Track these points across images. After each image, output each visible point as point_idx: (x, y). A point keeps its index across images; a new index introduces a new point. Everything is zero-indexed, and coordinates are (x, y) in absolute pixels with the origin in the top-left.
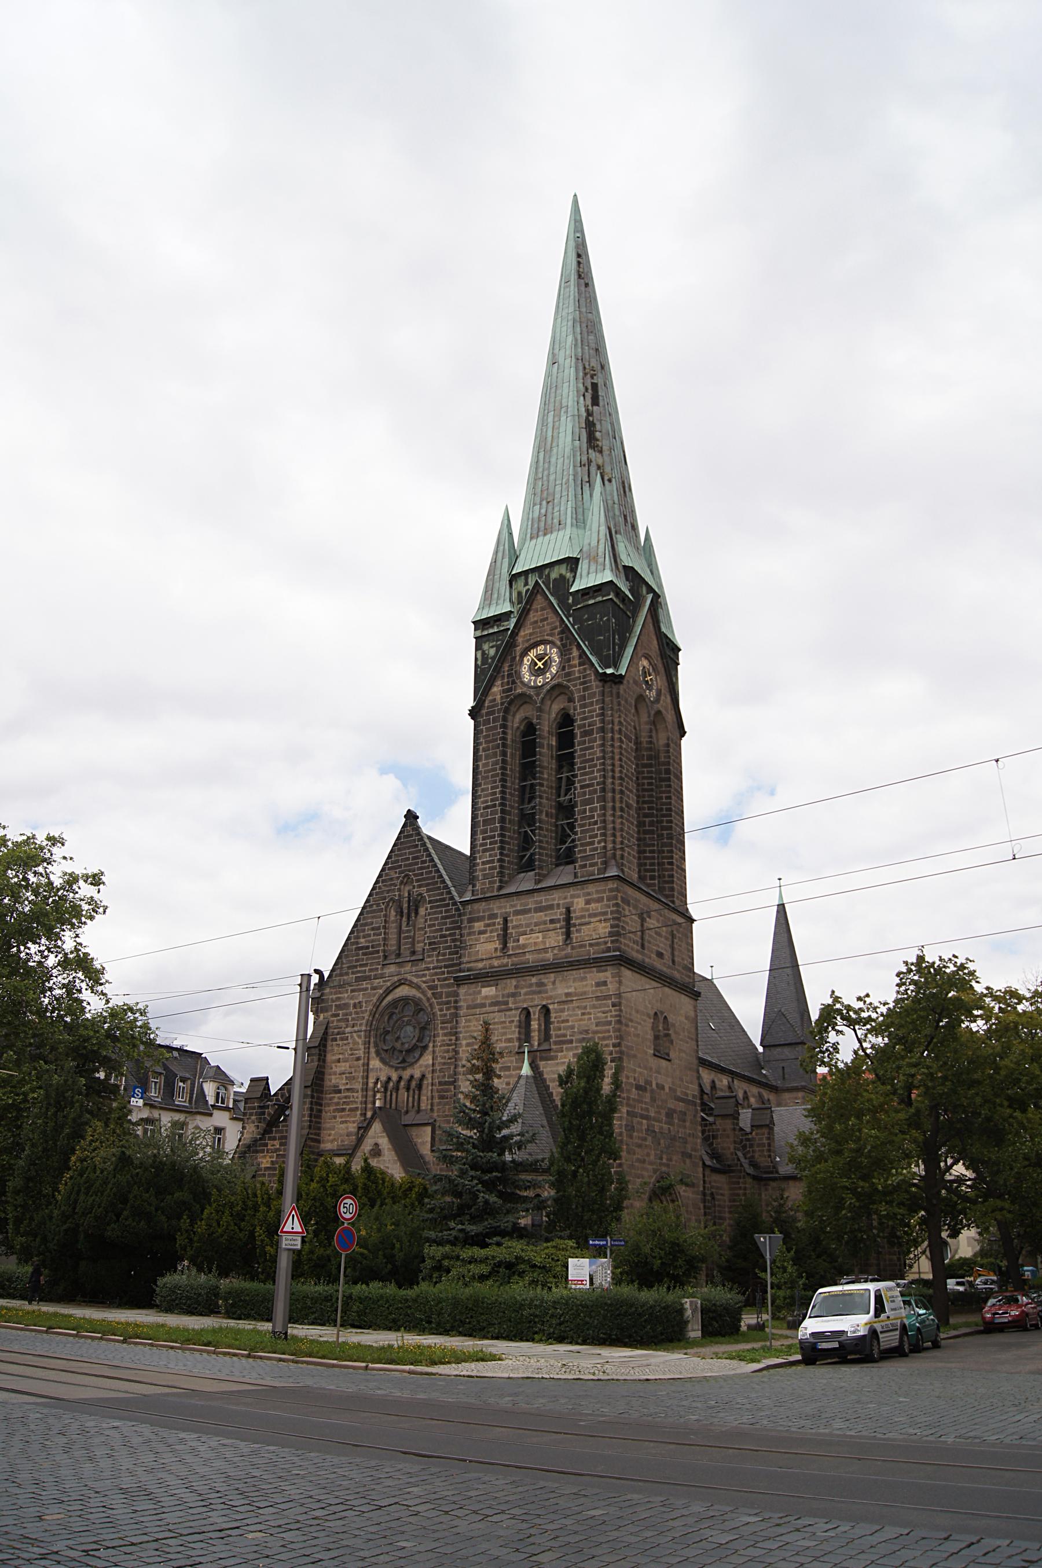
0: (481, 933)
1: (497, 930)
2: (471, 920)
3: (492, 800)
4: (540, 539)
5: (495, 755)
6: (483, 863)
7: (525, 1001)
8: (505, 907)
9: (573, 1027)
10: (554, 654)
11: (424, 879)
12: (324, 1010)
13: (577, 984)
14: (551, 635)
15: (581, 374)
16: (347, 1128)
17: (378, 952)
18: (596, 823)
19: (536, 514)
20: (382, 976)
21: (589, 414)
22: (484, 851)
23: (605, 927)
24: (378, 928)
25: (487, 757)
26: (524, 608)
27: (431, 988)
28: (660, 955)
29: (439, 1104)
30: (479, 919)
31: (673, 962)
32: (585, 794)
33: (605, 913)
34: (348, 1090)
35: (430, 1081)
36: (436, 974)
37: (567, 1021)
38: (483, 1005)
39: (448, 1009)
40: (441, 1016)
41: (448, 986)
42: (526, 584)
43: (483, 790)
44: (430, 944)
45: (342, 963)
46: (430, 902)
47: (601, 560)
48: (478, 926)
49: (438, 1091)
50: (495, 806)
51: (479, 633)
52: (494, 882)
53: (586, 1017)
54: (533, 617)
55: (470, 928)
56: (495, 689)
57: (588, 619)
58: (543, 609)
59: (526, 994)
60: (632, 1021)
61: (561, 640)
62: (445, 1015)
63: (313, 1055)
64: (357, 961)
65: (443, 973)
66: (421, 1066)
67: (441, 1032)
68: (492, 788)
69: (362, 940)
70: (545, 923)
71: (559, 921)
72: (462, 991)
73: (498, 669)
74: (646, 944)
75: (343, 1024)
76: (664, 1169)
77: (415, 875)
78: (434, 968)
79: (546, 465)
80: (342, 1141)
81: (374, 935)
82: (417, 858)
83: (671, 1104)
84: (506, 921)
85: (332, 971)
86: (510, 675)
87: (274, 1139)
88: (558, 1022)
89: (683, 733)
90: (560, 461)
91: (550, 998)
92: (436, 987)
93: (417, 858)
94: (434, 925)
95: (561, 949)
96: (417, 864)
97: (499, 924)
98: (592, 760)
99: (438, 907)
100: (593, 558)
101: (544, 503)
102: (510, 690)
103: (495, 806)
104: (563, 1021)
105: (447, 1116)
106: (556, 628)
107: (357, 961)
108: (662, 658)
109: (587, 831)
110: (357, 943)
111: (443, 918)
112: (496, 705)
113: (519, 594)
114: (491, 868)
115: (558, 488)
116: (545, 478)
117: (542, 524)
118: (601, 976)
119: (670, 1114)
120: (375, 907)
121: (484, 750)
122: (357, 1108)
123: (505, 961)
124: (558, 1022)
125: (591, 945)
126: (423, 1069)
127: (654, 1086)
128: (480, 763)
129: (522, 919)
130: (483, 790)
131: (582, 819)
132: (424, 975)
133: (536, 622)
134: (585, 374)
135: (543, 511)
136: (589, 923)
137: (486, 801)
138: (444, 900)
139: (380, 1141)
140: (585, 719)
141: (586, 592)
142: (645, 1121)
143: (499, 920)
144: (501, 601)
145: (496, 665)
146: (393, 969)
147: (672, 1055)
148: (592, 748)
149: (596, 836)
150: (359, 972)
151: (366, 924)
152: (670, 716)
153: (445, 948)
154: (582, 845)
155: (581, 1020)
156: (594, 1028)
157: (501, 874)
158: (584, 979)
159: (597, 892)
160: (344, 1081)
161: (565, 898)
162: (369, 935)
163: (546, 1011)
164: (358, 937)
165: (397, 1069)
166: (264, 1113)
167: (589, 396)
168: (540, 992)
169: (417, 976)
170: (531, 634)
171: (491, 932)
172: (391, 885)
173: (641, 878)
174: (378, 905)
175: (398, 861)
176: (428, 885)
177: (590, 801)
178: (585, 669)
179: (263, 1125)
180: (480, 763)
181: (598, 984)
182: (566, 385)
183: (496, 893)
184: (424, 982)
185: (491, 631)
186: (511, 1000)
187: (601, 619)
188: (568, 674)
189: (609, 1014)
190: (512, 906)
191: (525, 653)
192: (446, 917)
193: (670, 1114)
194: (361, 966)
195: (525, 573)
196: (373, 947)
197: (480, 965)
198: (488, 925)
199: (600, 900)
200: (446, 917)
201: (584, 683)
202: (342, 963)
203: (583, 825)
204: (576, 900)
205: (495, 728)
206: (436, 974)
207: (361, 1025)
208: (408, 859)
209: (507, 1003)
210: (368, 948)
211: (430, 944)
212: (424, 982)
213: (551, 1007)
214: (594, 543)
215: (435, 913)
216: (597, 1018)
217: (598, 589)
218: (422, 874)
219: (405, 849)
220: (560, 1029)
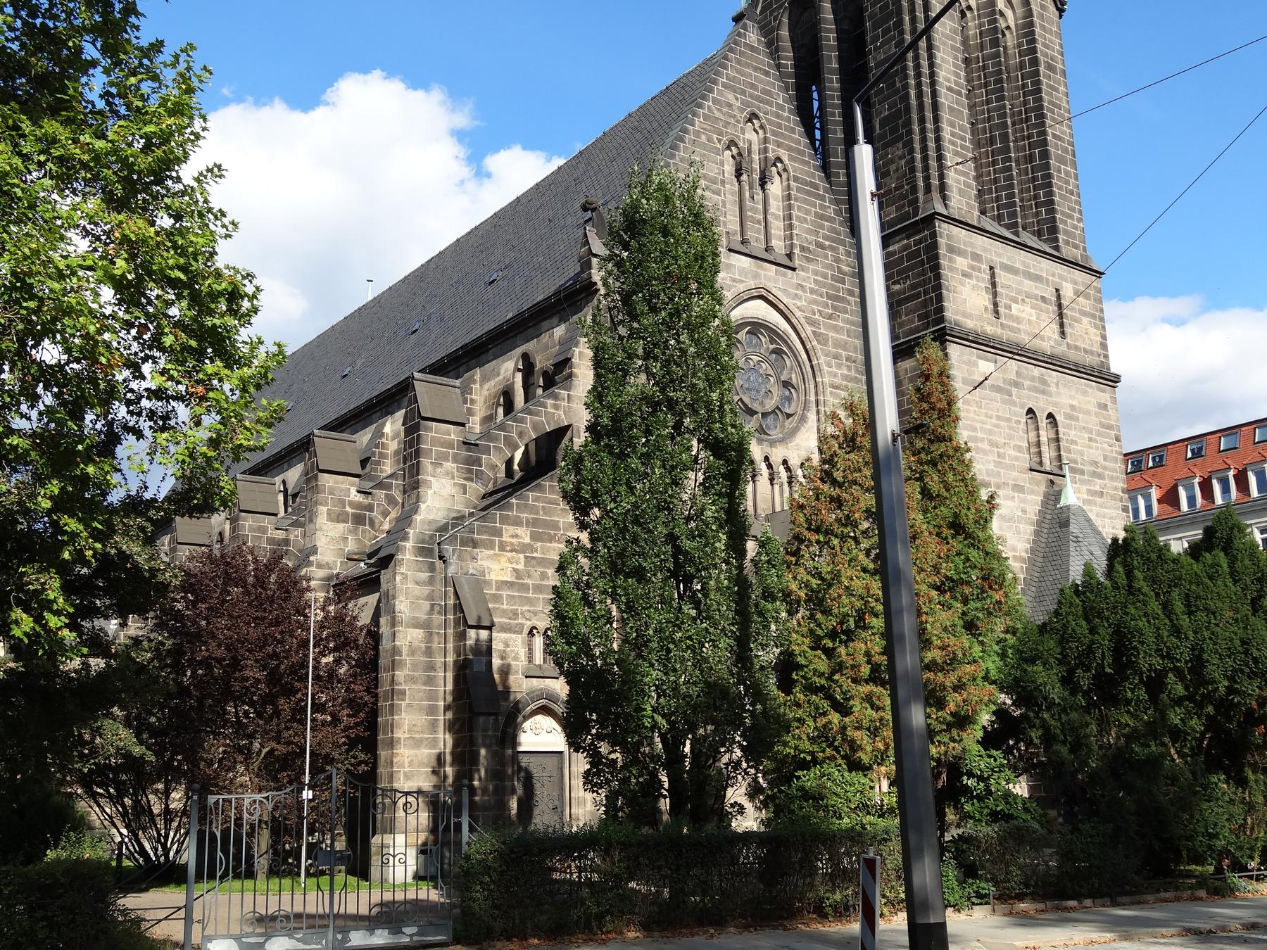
7: (1029, 398)
13: (1080, 397)
27: (812, 323)
30: (961, 253)
36: (815, 302)
41: (836, 329)
46: (796, 179)
78: (812, 291)
87: (517, 523)
123: (999, 331)
136: (1079, 321)
138: (816, 187)
156: (1101, 459)
158: (1085, 393)
168: (1043, 392)
206: (815, 302)
211: (803, 249)
215: (805, 201)
219: (749, 66)
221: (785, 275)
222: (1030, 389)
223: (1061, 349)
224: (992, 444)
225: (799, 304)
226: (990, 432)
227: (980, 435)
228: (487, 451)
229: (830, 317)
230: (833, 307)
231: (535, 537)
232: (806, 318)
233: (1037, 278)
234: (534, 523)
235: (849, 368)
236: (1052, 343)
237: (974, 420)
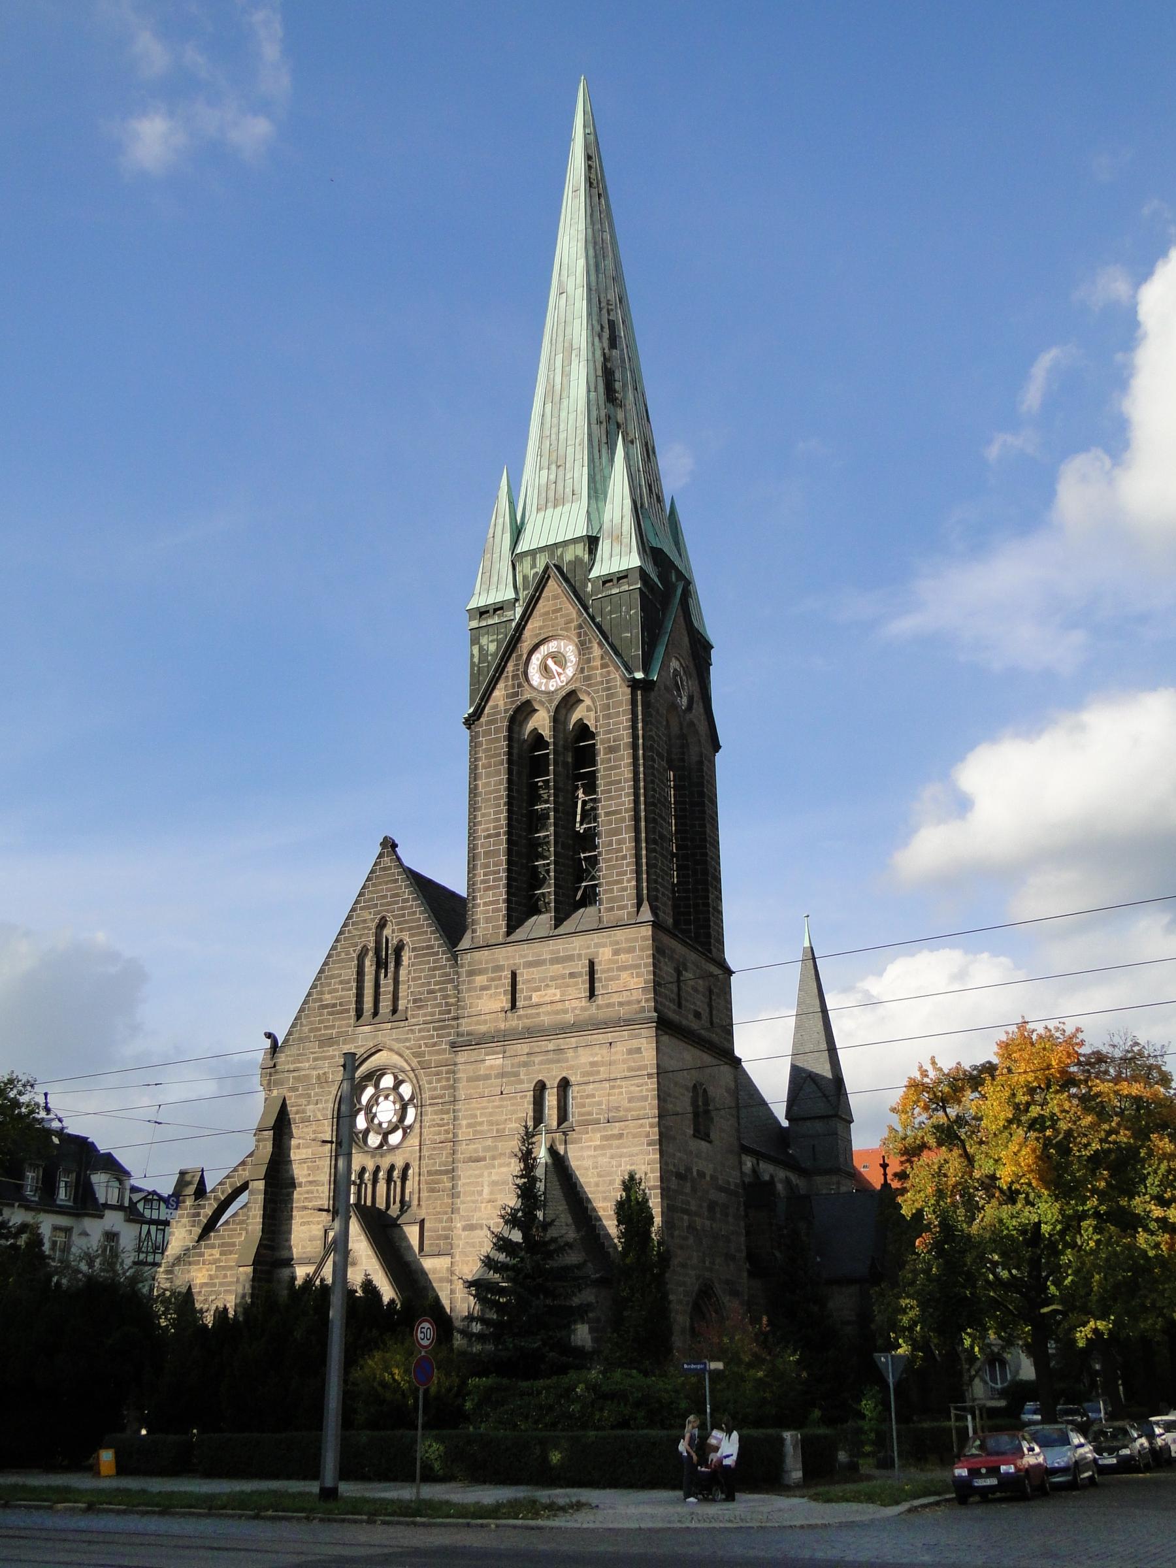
0: (483, 988)
1: (504, 985)
2: (471, 973)
3: (495, 828)
4: (550, 511)
5: (498, 773)
6: (485, 904)
7: (540, 1071)
8: (514, 957)
9: (600, 1103)
10: (570, 651)
11: (406, 922)
12: (278, 1083)
14: (567, 629)
15: (595, 310)
17: (348, 1011)
18: (624, 857)
19: (544, 481)
21: (606, 360)
22: (487, 889)
23: (637, 983)
24: (348, 982)
25: (488, 776)
26: (533, 597)
28: (697, 1015)
29: (429, 1198)
30: (480, 972)
31: (712, 1023)
32: (610, 822)
33: (638, 966)
34: (310, 1182)
35: (417, 1170)
36: (423, 1038)
37: (593, 1096)
38: (487, 1077)
39: (438, 1081)
40: (430, 1089)
41: (438, 1052)
42: (533, 566)
43: (483, 815)
44: (415, 1001)
45: (302, 1025)
46: (414, 949)
47: (626, 541)
48: (480, 980)
50: (498, 835)
51: (474, 624)
52: (499, 927)
53: (617, 1091)
54: (542, 606)
55: (469, 982)
56: (496, 693)
57: (611, 612)
58: (556, 597)
59: (541, 1063)
60: (669, 1095)
61: (579, 635)
62: (435, 1089)
63: (265, 1140)
64: (321, 1022)
65: (433, 1036)
68: (496, 813)
69: (327, 996)
70: (563, 977)
71: (580, 974)
72: (462, 1057)
73: (500, 670)
74: (683, 1002)
75: (303, 1101)
76: (707, 1274)
77: (395, 917)
79: (555, 420)
80: (304, 1247)
81: (343, 989)
82: (397, 895)
83: (714, 1195)
84: (514, 975)
85: (290, 1033)
86: (515, 677)
87: (213, 1247)
88: (582, 1097)
89: (717, 747)
90: (572, 417)
91: (570, 1068)
93: (397, 895)
94: (420, 978)
95: (583, 1009)
96: (397, 903)
97: (506, 977)
98: (619, 782)
99: (424, 955)
100: (617, 538)
101: (553, 467)
102: (516, 694)
103: (498, 835)
104: (588, 1096)
105: (439, 1213)
106: (571, 621)
107: (321, 1022)
108: (694, 659)
109: (614, 867)
110: (321, 1000)
111: (431, 969)
112: (498, 713)
113: (525, 577)
114: (494, 911)
115: (570, 450)
116: (553, 437)
117: (551, 494)
118: (635, 1043)
119: (712, 1206)
120: (343, 956)
121: (484, 767)
123: (514, 1023)
124: (582, 1097)
125: (621, 1004)
126: (407, 1155)
127: (695, 1173)
128: (479, 783)
129: (535, 973)
130: (483, 815)
131: (608, 852)
132: (408, 1040)
133: (547, 613)
134: (601, 309)
135: (552, 477)
136: (618, 978)
137: (488, 829)
138: (431, 947)
140: (610, 731)
141: (607, 580)
142: (685, 1217)
143: (507, 973)
144: (502, 586)
145: (499, 664)
147: (713, 1136)
148: (619, 767)
149: (625, 873)
151: (332, 977)
152: (702, 728)
153: (434, 1006)
154: (608, 883)
155: (609, 1095)
156: (626, 1104)
157: (509, 917)
159: (627, 940)
160: (306, 1172)
161: (588, 948)
162: (336, 990)
163: (564, 1084)
164: (322, 993)
165: (373, 1156)
166: (198, 1215)
167: (606, 334)
168: (558, 1061)
169: (398, 1040)
170: (541, 628)
171: (497, 987)
172: (364, 928)
173: (676, 923)
174: (348, 953)
175: (372, 899)
176: (410, 929)
177: (617, 832)
178: (609, 673)
179: (198, 1230)
180: (479, 783)
181: (630, 1052)
182: (577, 322)
183: (501, 940)
184: (408, 1048)
185: (490, 622)
186: (522, 1070)
187: (628, 612)
188: (588, 678)
189: (645, 1088)
190: (521, 956)
191: (536, 647)
192: (434, 969)
193: (712, 1206)
194: (326, 1028)
195: (533, 553)
196: (341, 1004)
197: (483, 1028)
198: (493, 979)
199: (630, 950)
200: (434, 969)
201: (608, 689)
202: (302, 1025)
203: (610, 860)
204: (601, 950)
205: (497, 740)
206: (423, 1038)
207: (326, 1101)
208: (385, 897)
209: (517, 1074)
210: (334, 1005)
211: (415, 1001)
212: (408, 1048)
213: (572, 1079)
214: (617, 520)
216: (631, 1093)
217: (622, 576)
218: (403, 915)
219: (380, 884)
220: (584, 1106)
222: (541, 1063)
223: (593, 1010)
224: (491, 1123)
226: (491, 1114)
227: (479, 1120)
228: (203, 1207)
229: (435, 1045)
230: (438, 1036)
232: (413, 1053)
233: (570, 958)
234: (222, 1245)
235: (448, 1079)
236: (577, 1012)
237: (474, 1109)
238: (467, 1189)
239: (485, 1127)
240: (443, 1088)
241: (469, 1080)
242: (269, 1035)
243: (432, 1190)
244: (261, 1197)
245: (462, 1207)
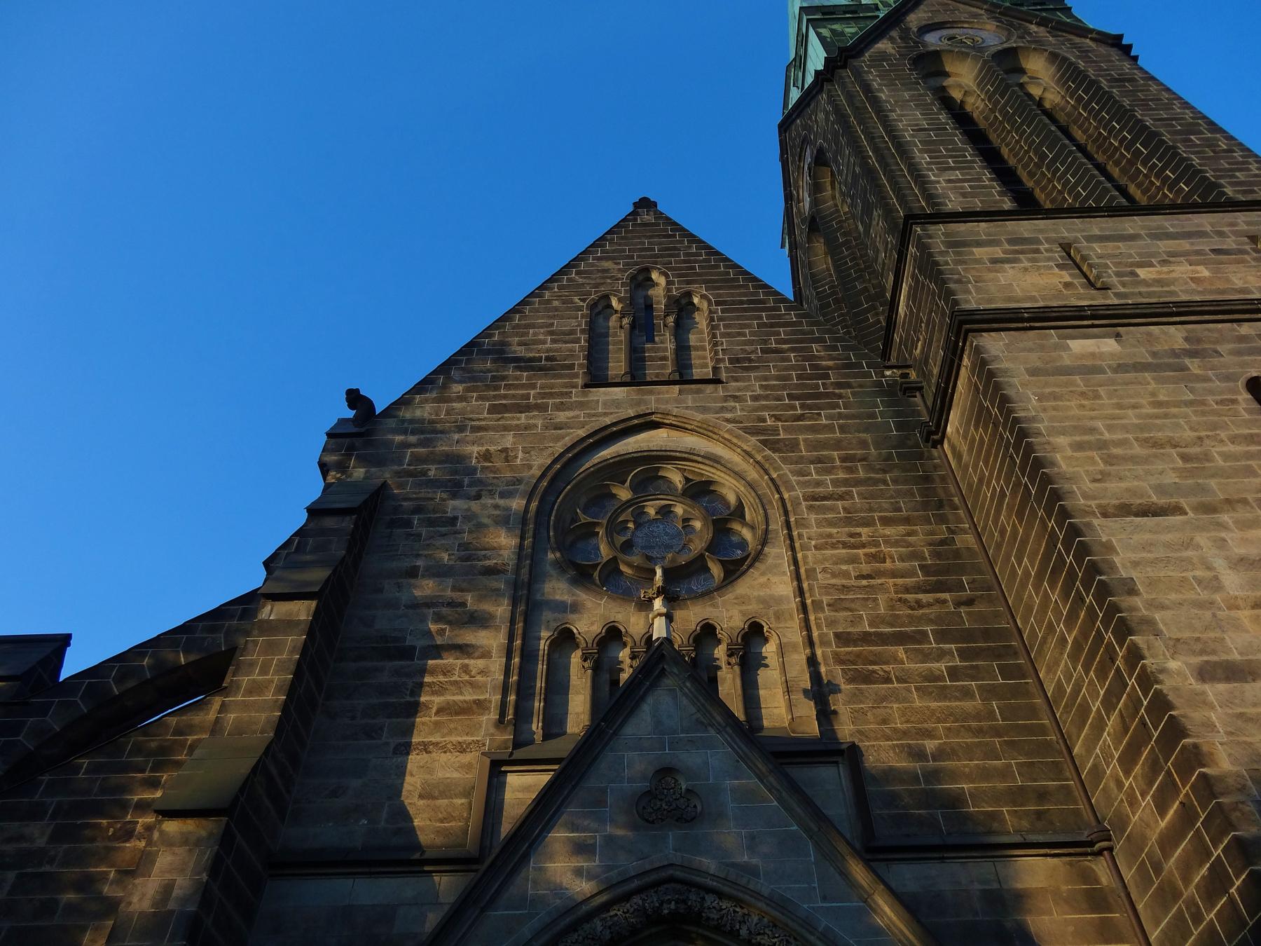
16: (430, 771)
20: (581, 405)
24: (572, 332)
39: (829, 471)
49: (839, 660)
62: (818, 484)
66: (742, 600)
67: (813, 517)
78: (755, 398)
81: (554, 341)
92: (775, 431)
105: (905, 734)
122: (481, 705)
126: (753, 607)
139: (690, 758)
146: (619, 393)
150: (505, 397)
176: (705, 282)
221: (698, 392)
225: (728, 416)
231: (56, 838)
235: (850, 470)
238: (1151, 572)
239: (1137, 450)
240: (836, 483)
241: (1033, 372)
242: (354, 398)
243: (868, 678)
244: (293, 642)
245: (1157, 616)
